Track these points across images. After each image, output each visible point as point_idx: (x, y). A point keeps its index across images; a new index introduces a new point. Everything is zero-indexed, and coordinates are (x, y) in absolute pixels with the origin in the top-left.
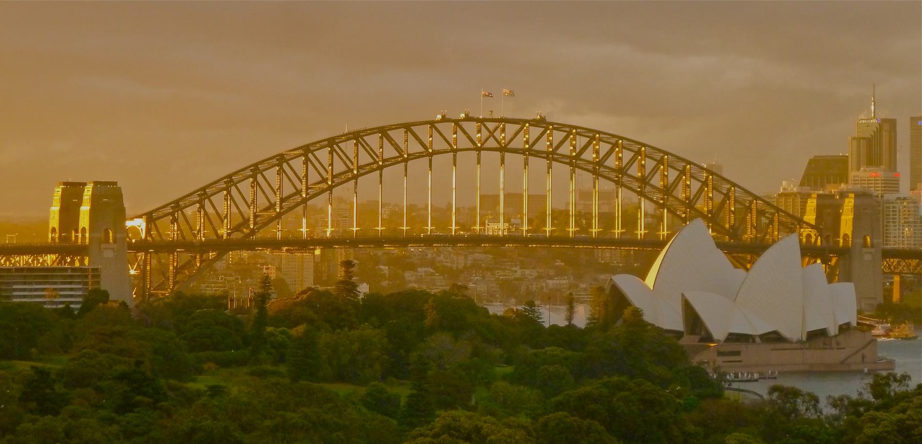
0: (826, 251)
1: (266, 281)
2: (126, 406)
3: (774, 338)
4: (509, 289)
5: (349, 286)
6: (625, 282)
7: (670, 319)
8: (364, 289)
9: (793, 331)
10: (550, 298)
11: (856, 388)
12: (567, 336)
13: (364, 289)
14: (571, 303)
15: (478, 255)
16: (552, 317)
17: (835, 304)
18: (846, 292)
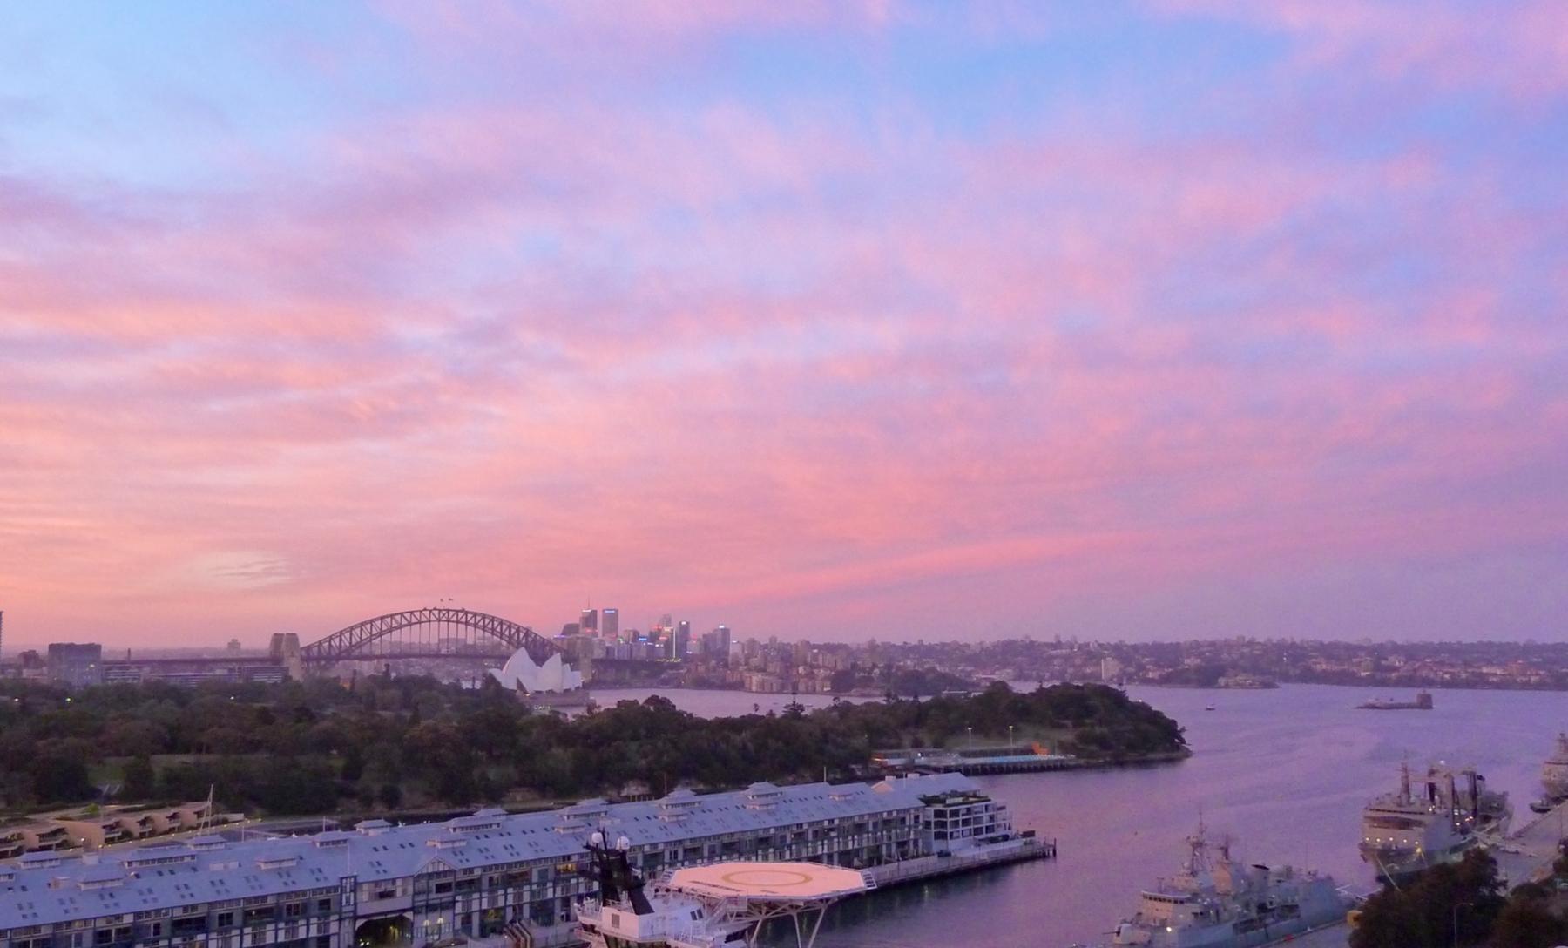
0: (570, 659)
1: (355, 672)
2: (299, 720)
3: (551, 692)
4: (450, 674)
5: (387, 673)
6: (496, 672)
7: (510, 685)
8: (393, 675)
9: (558, 690)
10: (466, 678)
11: (582, 711)
12: (472, 692)
13: (393, 675)
14: (474, 679)
15: (438, 661)
16: (466, 685)
17: (576, 679)
18: (577, 673)
